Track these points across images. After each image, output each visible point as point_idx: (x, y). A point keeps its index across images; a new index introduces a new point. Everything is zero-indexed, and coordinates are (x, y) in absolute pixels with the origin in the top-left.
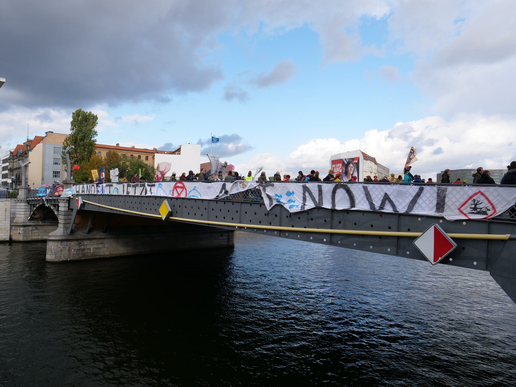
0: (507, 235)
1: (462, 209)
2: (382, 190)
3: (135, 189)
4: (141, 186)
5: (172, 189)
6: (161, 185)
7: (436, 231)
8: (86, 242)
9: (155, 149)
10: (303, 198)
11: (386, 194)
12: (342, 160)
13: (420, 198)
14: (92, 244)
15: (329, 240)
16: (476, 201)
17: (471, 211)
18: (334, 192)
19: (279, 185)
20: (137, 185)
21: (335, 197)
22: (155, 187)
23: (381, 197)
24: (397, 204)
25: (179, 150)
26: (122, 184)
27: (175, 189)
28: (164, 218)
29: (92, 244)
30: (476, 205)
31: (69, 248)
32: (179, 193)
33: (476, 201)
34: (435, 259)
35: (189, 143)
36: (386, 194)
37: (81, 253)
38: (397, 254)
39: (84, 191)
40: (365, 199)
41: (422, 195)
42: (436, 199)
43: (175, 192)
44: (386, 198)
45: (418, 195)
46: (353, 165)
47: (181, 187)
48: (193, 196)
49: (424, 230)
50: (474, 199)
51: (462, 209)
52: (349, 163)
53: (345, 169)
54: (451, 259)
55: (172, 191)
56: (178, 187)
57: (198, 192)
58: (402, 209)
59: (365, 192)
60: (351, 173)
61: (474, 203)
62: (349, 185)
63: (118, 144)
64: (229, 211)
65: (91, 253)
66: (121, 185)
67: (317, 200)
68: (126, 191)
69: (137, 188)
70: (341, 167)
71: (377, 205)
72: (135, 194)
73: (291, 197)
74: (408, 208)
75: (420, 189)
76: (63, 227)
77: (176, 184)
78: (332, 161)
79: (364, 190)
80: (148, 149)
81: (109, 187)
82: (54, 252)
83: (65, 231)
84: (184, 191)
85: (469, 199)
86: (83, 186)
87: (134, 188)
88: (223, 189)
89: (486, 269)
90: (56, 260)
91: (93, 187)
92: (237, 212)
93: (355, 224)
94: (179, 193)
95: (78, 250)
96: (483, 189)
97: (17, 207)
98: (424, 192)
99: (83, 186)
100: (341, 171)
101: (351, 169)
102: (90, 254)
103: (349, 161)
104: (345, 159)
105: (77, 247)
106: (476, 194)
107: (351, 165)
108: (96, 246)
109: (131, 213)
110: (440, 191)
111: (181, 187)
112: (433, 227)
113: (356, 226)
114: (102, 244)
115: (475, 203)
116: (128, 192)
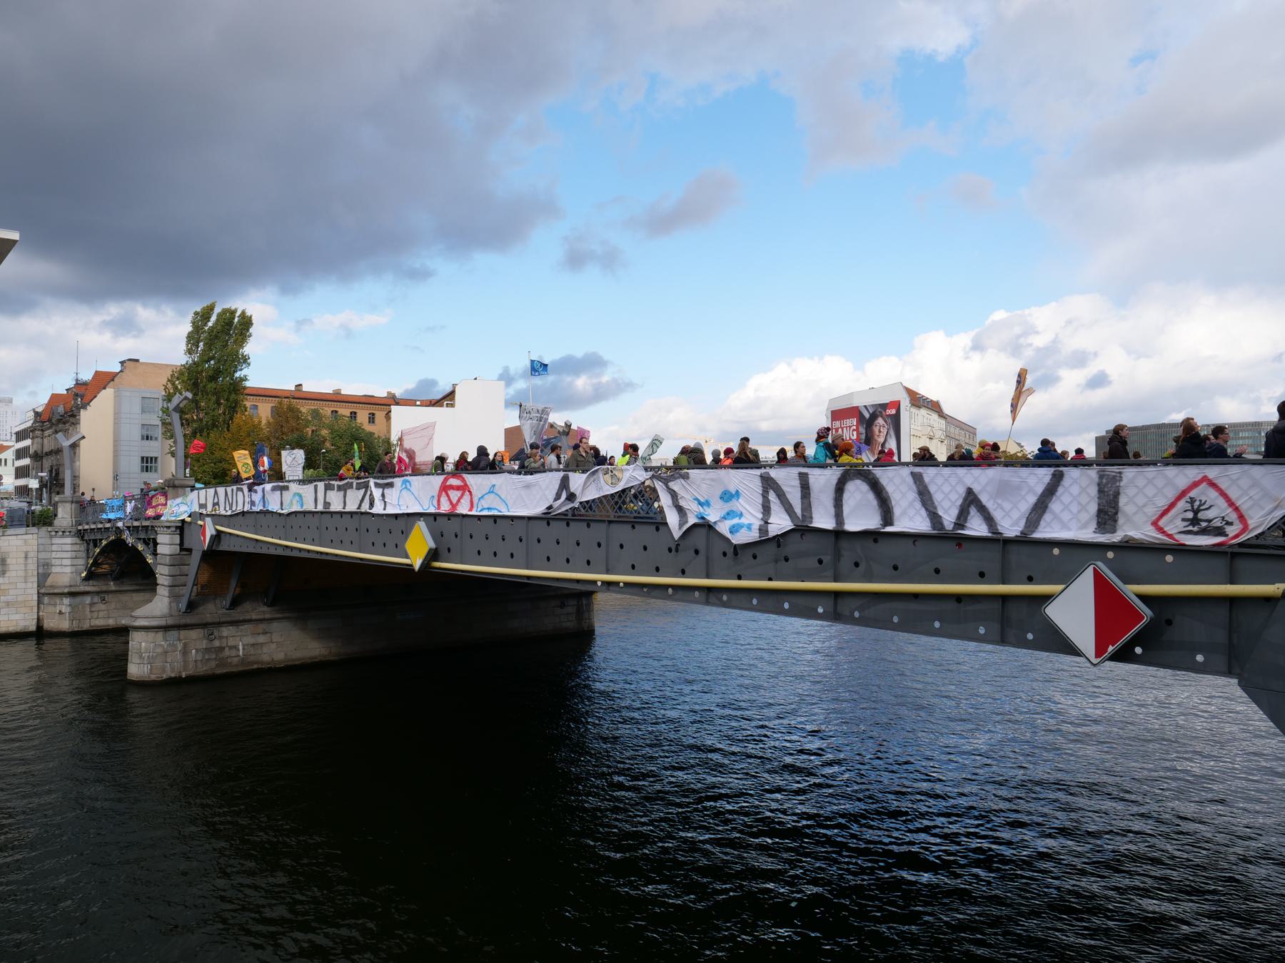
0: (1277, 585)
1: (1161, 523)
2: (960, 481)
3: (345, 497)
4: (358, 489)
6: (408, 484)
7: (1099, 579)
8: (225, 631)
9: (391, 396)
10: (763, 506)
11: (970, 491)
12: (857, 408)
13: (1054, 498)
14: (239, 634)
15: (831, 609)
16: (1197, 503)
17: (1184, 527)
19: (703, 476)
20: (350, 486)
21: (841, 500)
22: (394, 489)
23: (957, 498)
24: (997, 515)
25: (450, 397)
26: (312, 482)
27: (443, 493)
28: (417, 566)
29: (239, 634)
30: (1196, 512)
31: (185, 646)
32: (455, 502)
33: (1197, 503)
34: (1100, 651)
35: (476, 379)
36: (970, 491)
37: (214, 657)
38: (1003, 641)
39: (217, 504)
40: (918, 505)
41: (1060, 490)
42: (1097, 500)
43: (444, 499)
44: (971, 500)
45: (1050, 491)
46: (886, 422)
47: (458, 488)
48: (489, 509)
49: (1066, 578)
50: (1191, 498)
51: (1161, 523)
52: (874, 417)
53: (864, 432)
54: (1138, 650)
55: (436, 498)
56: (452, 487)
57: (501, 498)
58: (1011, 527)
59: (918, 487)
60: (881, 440)
61: (1192, 506)
62: (878, 472)
63: (301, 385)
64: (578, 544)
65: (239, 656)
66: (311, 487)
67: (798, 511)
68: (322, 501)
69: (349, 492)
70: (855, 428)
71: (949, 518)
72: (344, 508)
74: (1026, 523)
75: (1054, 475)
76: (167, 595)
77: (446, 480)
78: (833, 412)
79: (915, 483)
80: (373, 396)
81: (279, 492)
82: (146, 658)
83: (174, 605)
84: (467, 496)
85: (1179, 498)
86: (216, 492)
87: (342, 493)
88: (562, 491)
89: (1229, 673)
90: (153, 677)
91: (240, 494)
92: (599, 545)
93: (895, 568)
94: (455, 502)
95: (207, 650)
96: (1212, 472)
97: (54, 548)
98: (1066, 482)
99: (216, 492)
100: (855, 437)
101: (880, 432)
102: (236, 660)
103: (873, 412)
104: (865, 406)
105: (204, 644)
106: (1195, 485)
107: (880, 421)
108: (250, 640)
109: (336, 555)
110: (1104, 481)
111: (458, 488)
112: (1090, 572)
113: (897, 572)
114: (265, 633)
115: (1195, 507)
116: (327, 504)
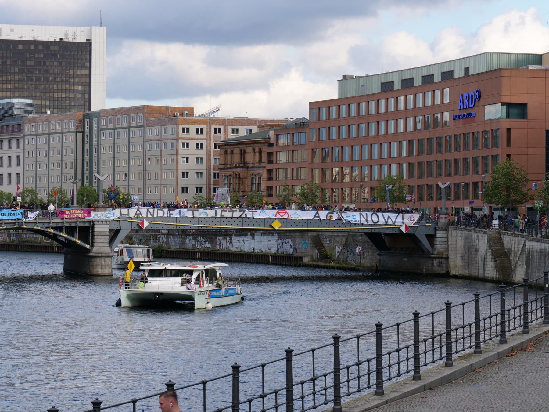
4: (239, 211)
5: (275, 213)
18: (372, 215)
39: (140, 214)
44: (389, 217)
69: (234, 213)
73: (355, 217)
87: (231, 213)
96: (412, 215)
